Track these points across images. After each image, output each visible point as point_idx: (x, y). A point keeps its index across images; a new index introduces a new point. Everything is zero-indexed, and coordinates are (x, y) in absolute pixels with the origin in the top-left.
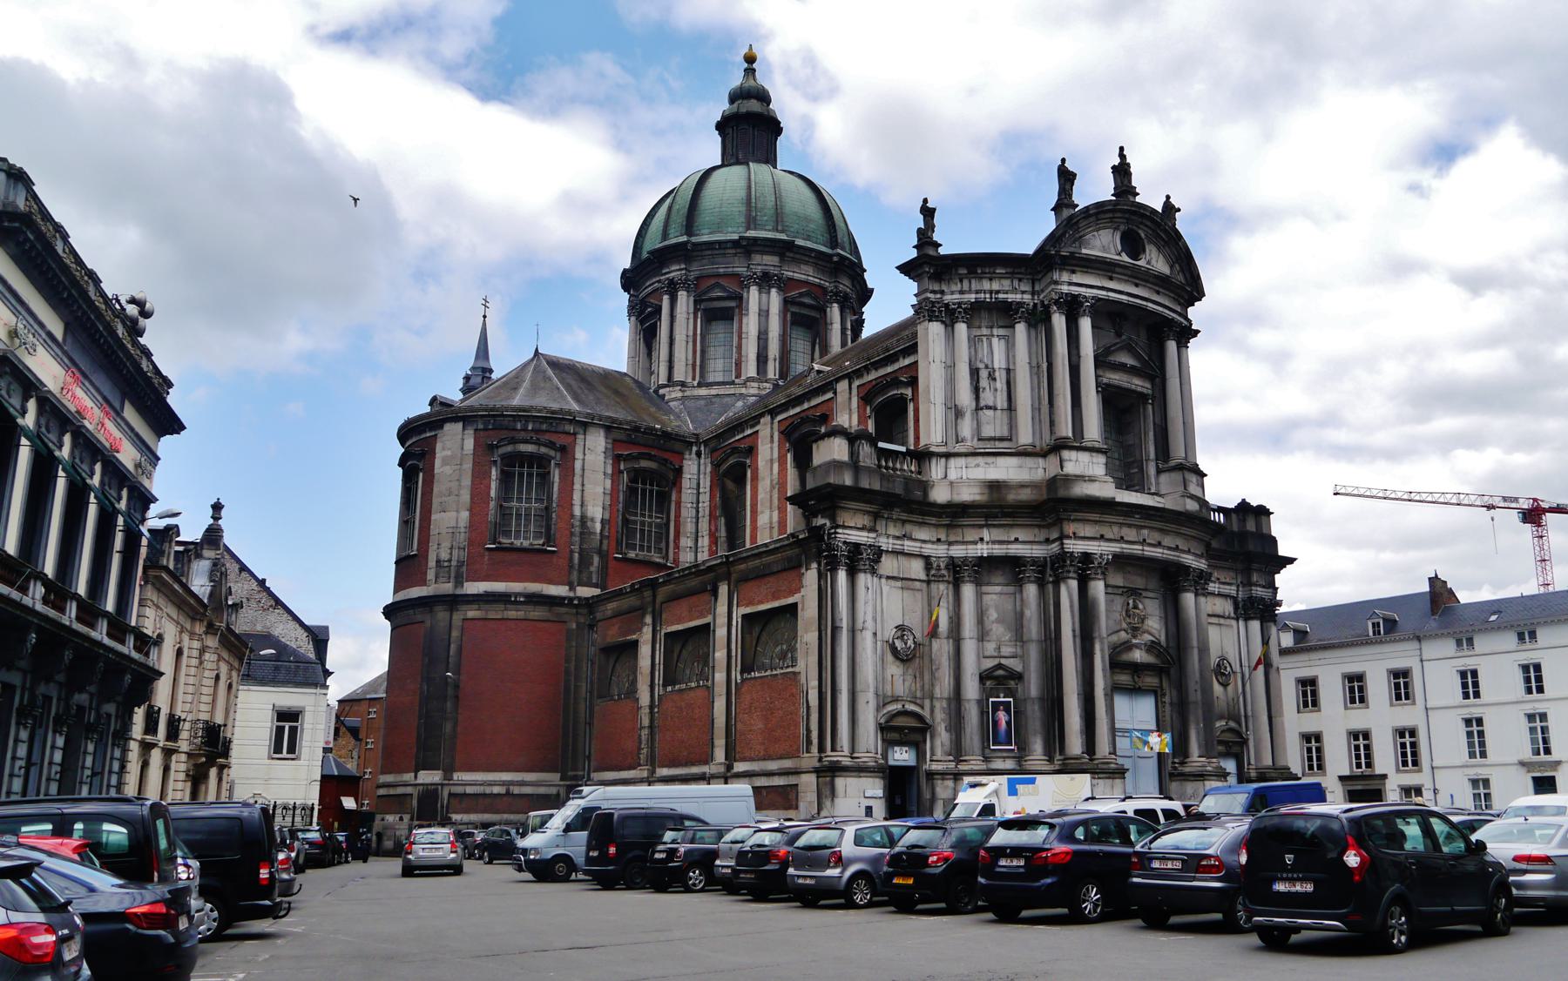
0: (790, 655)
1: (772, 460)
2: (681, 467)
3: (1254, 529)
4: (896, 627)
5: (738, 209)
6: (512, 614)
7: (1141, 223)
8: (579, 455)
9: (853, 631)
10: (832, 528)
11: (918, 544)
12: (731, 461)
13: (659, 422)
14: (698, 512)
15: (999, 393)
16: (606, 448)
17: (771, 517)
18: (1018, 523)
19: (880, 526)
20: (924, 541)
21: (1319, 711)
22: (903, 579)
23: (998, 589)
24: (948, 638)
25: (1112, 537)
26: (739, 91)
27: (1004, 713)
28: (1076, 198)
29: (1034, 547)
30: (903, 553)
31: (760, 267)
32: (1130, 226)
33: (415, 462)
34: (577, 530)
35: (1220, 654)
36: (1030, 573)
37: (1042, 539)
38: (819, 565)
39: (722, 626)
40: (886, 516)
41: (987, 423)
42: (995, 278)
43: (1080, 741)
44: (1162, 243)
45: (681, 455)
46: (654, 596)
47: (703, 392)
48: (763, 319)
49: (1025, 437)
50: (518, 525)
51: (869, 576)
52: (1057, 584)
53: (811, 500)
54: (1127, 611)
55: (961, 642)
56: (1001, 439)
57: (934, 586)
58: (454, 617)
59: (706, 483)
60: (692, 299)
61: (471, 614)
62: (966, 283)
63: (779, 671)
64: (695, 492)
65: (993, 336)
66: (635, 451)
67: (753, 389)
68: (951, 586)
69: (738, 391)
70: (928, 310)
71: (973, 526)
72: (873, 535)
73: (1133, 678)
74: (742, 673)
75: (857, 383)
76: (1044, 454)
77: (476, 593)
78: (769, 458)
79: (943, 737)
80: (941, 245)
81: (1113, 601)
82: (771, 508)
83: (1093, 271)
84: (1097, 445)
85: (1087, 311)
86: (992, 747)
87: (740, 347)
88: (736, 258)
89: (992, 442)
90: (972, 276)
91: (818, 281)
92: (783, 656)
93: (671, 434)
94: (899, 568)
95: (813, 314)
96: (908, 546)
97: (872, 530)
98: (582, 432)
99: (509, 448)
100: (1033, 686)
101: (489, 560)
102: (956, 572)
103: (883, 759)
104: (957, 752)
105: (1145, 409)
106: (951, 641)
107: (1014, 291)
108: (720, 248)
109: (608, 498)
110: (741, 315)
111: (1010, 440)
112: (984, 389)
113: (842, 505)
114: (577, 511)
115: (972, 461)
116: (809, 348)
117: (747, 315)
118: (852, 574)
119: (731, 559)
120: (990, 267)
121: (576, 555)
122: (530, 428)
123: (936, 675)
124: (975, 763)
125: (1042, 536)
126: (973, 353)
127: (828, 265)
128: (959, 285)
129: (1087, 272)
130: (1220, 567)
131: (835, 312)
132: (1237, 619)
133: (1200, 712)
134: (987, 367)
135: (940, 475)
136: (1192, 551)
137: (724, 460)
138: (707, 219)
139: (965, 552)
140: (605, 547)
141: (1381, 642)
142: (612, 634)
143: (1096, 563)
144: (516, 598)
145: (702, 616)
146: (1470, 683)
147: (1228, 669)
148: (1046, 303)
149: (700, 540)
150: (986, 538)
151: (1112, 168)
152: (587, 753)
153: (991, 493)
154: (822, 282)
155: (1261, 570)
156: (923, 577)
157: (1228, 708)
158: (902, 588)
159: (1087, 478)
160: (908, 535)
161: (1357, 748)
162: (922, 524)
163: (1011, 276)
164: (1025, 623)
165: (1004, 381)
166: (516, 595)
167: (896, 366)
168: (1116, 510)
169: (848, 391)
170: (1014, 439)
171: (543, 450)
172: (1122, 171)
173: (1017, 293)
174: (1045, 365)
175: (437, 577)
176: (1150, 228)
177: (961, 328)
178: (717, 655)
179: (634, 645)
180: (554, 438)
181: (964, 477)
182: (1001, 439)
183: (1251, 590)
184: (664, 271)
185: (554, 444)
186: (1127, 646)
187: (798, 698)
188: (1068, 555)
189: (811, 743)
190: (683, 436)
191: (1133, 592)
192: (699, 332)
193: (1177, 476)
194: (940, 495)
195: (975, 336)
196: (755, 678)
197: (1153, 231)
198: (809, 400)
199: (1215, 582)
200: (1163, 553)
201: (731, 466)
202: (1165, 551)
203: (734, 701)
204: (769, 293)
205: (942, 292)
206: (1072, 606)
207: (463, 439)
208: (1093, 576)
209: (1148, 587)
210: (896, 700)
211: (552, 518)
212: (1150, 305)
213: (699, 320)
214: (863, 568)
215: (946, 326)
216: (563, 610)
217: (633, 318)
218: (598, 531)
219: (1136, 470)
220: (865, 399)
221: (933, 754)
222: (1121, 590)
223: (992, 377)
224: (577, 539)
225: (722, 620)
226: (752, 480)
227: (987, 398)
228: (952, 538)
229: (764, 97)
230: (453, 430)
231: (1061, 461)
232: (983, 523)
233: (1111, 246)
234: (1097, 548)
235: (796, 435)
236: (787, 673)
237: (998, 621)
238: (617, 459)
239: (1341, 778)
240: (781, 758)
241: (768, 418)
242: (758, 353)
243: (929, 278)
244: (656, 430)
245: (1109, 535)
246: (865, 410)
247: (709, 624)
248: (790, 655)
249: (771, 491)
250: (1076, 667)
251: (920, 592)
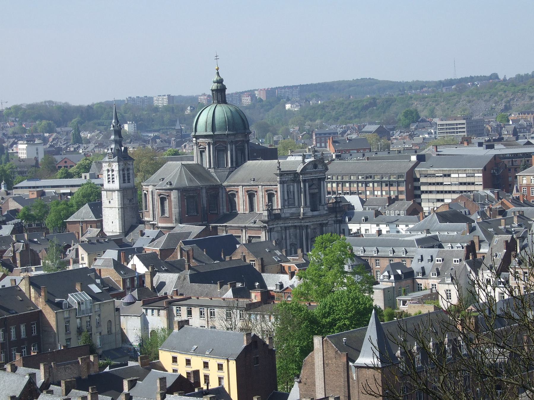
8: (201, 194)
59: (224, 195)
114: (202, 206)
145: (238, 234)
171: (195, 194)
177: (285, 185)
227: (290, 196)
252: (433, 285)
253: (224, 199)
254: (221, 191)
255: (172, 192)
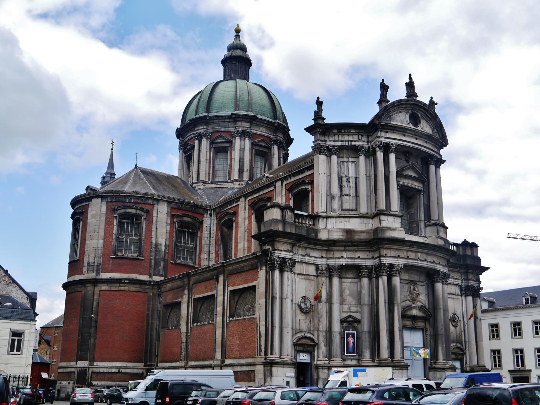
0: (252, 310)
1: (245, 218)
2: (203, 221)
3: (470, 254)
4: (302, 297)
5: (231, 101)
6: (123, 288)
7: (419, 110)
8: (155, 214)
9: (282, 299)
10: (272, 250)
11: (313, 259)
12: (226, 218)
13: (193, 200)
14: (210, 242)
15: (351, 188)
16: (168, 212)
17: (244, 245)
18: (360, 249)
19: (295, 250)
20: (315, 257)
21: (500, 339)
22: (305, 275)
23: (350, 280)
24: (326, 303)
25: (404, 257)
26: (232, 46)
27: (352, 338)
28: (389, 98)
29: (367, 261)
30: (305, 263)
31: (240, 128)
32: (414, 111)
33: (79, 216)
34: (154, 249)
35: (454, 312)
37: (371, 257)
38: (266, 268)
39: (221, 295)
40: (298, 245)
41: (346, 202)
42: (350, 134)
43: (387, 352)
44: (429, 119)
45: (202, 215)
46: (189, 281)
47: (213, 186)
48: (242, 152)
49: (363, 209)
50: (126, 247)
51: (289, 273)
52: (377, 278)
53: (263, 237)
54: (410, 291)
55: (332, 304)
56: (352, 210)
57: (320, 278)
58: (96, 289)
59: (214, 228)
60: (209, 142)
61: (103, 288)
62: (337, 136)
63: (247, 317)
64: (209, 232)
65: (349, 161)
66: (181, 213)
67: (236, 185)
68: (328, 279)
69: (229, 186)
70: (319, 149)
71: (339, 250)
72: (292, 254)
73: (412, 322)
74: (229, 317)
75: (285, 183)
76: (372, 217)
77: (106, 278)
78: (244, 217)
79: (323, 350)
80: (325, 119)
81: (403, 286)
82: (244, 241)
83: (396, 132)
84: (397, 213)
85: (393, 151)
86: (346, 354)
87: (231, 165)
88: (230, 123)
89: (348, 211)
90: (340, 133)
91: (268, 135)
92: (249, 310)
93: (198, 205)
94: (303, 269)
95: (265, 150)
96: (308, 259)
97: (291, 251)
98: (156, 203)
99: (123, 211)
100: (366, 326)
101: (112, 263)
102: (330, 272)
103: (295, 359)
104: (330, 356)
105: (420, 197)
106: (327, 304)
107: (359, 140)
108: (222, 119)
109: (168, 235)
110: (232, 150)
111: (357, 210)
112: (345, 186)
113: (278, 240)
114: (154, 241)
115: (338, 220)
116: (263, 166)
117: (234, 150)
118: (282, 272)
119: (225, 264)
120: (348, 129)
121: (153, 261)
122: (132, 201)
123: (320, 320)
124: (339, 362)
125: (371, 255)
126: (340, 170)
127: (273, 127)
128: (333, 137)
129: (393, 132)
130: (454, 271)
131: (275, 149)
132: (462, 296)
133: (444, 339)
134: (346, 176)
135: (324, 226)
136: (441, 263)
137: (223, 218)
138: (216, 105)
139: (334, 262)
140: (166, 258)
141: (529, 307)
142: (169, 298)
143: (396, 269)
144: (124, 281)
145: (211, 291)
147: (457, 319)
148: (374, 146)
149: (211, 255)
150: (345, 256)
151: (406, 84)
152: (156, 354)
153: (347, 235)
154: (270, 135)
155: (473, 273)
156: (315, 274)
157: (457, 336)
158: (305, 279)
159: (392, 229)
160: (308, 254)
161: (517, 357)
162: (315, 249)
163: (358, 134)
164: (362, 296)
165: (354, 183)
166: (125, 279)
167: (304, 175)
168: (405, 244)
169: (281, 186)
170: (358, 210)
171: (138, 212)
172: (410, 85)
173: (361, 142)
174: (373, 176)
175: (88, 271)
176: (423, 112)
177: (334, 158)
178: (218, 309)
179: (179, 304)
180: (143, 206)
181: (335, 228)
182: (352, 210)
183: (468, 282)
184: (196, 129)
185: (144, 209)
186: (410, 308)
187: (256, 330)
188: (383, 264)
189: (261, 351)
190: (204, 207)
191: (413, 282)
192: (212, 158)
193: (434, 228)
194: (323, 236)
195: (341, 162)
196: (235, 320)
197: (425, 113)
198: (263, 190)
199: (451, 278)
200: (427, 264)
201: (226, 221)
202: (428, 264)
203: (225, 330)
204: (245, 140)
205: (326, 141)
206: (384, 289)
207: (101, 206)
208: (394, 275)
209: (420, 280)
210: (301, 331)
211: (142, 244)
212: (423, 148)
213: (212, 152)
214: (286, 269)
215: (327, 157)
216: (146, 287)
217: (181, 151)
218: (163, 250)
219: (415, 225)
220: (289, 190)
221: (318, 357)
222: (407, 281)
223: (348, 181)
224: (153, 254)
225: (220, 293)
226: (235, 228)
227: (346, 190)
228: (328, 256)
229: (244, 49)
230: (96, 202)
231: (380, 221)
232: (343, 249)
233: (405, 120)
234: (396, 262)
235: (256, 207)
236: (250, 318)
237: (349, 295)
238: (173, 216)
239: (510, 371)
240: (247, 358)
241: (243, 199)
242: (239, 168)
243: (320, 134)
244: (191, 203)
245: (401, 256)
246: (289, 195)
247: (214, 294)
248: (252, 310)
249: (244, 233)
250: (386, 317)
251: (313, 281)
253: (213, 239)
254: (207, 220)
255: (90, 203)
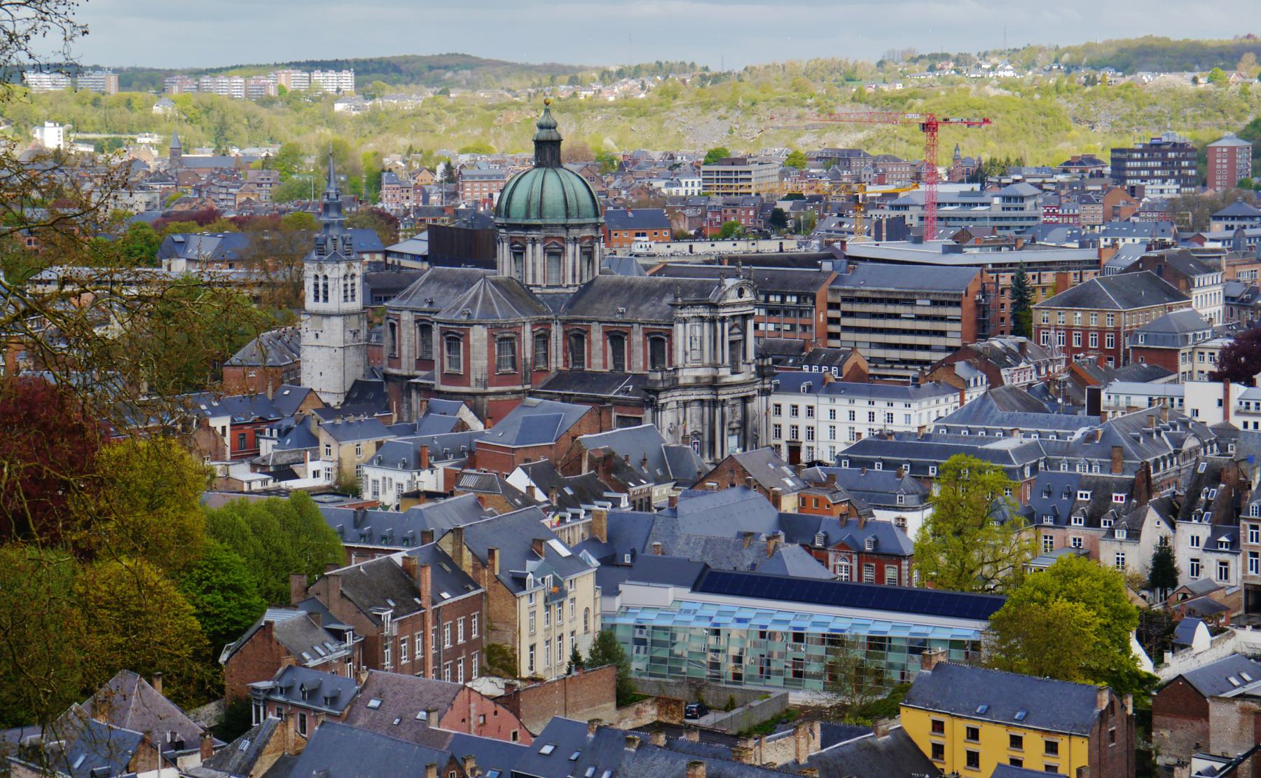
36: (707, 404)
59: (560, 337)
67: (571, 290)
125: (710, 392)
146: (833, 413)
194: (681, 381)
227: (694, 347)
252: (1075, 540)
